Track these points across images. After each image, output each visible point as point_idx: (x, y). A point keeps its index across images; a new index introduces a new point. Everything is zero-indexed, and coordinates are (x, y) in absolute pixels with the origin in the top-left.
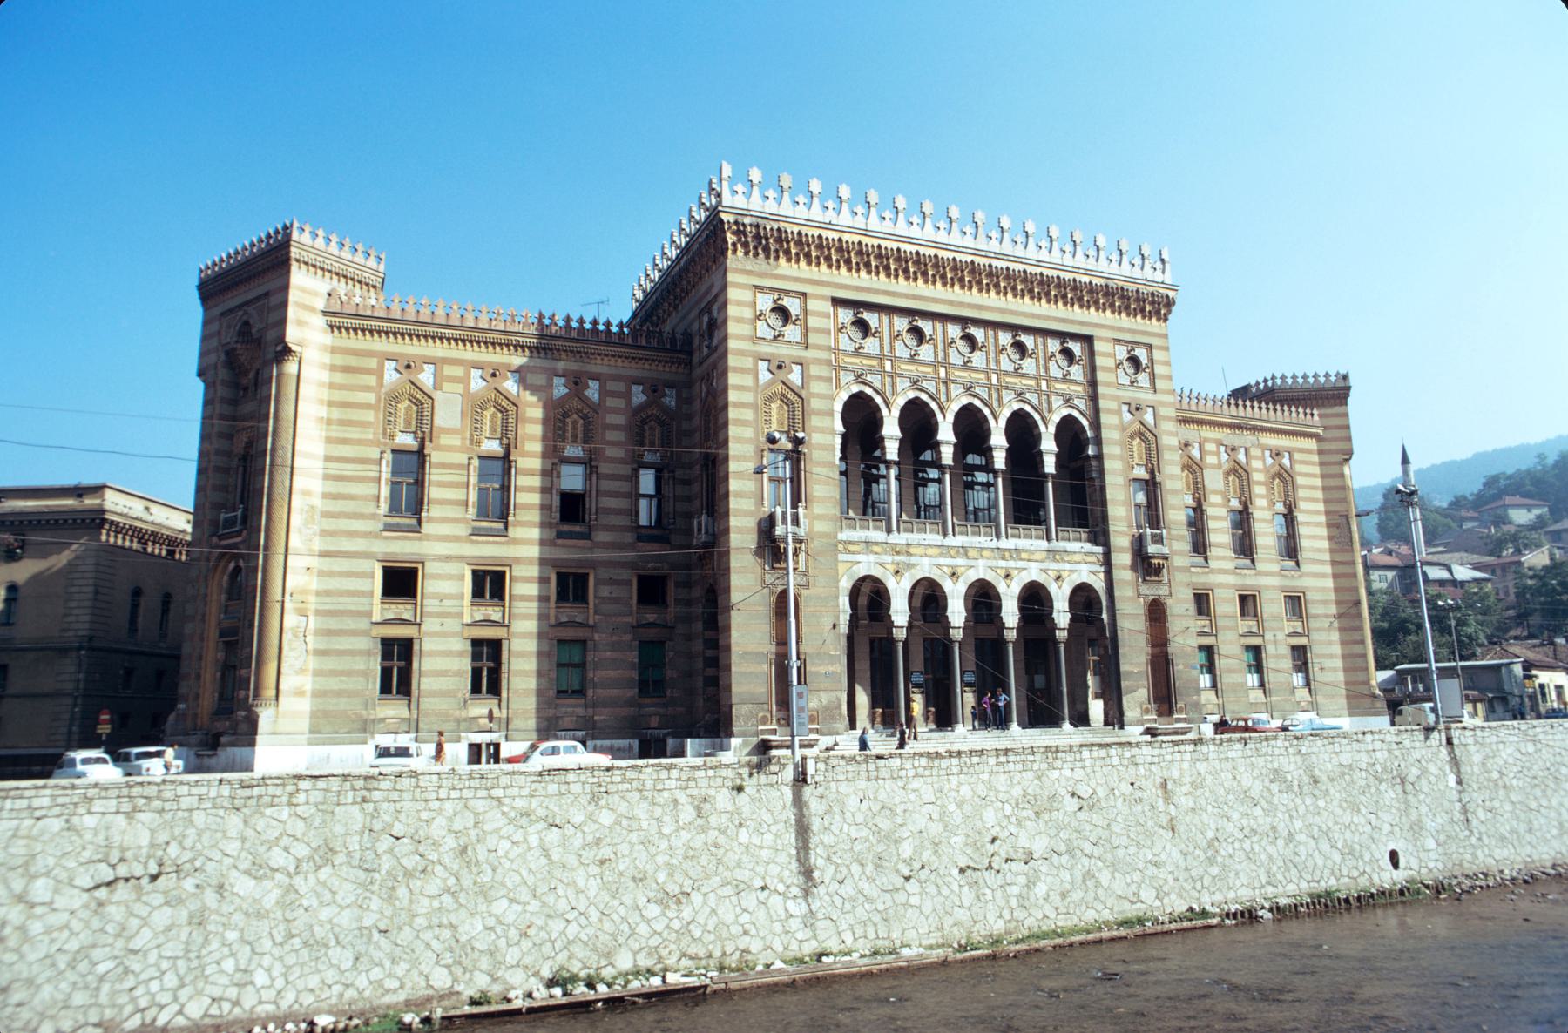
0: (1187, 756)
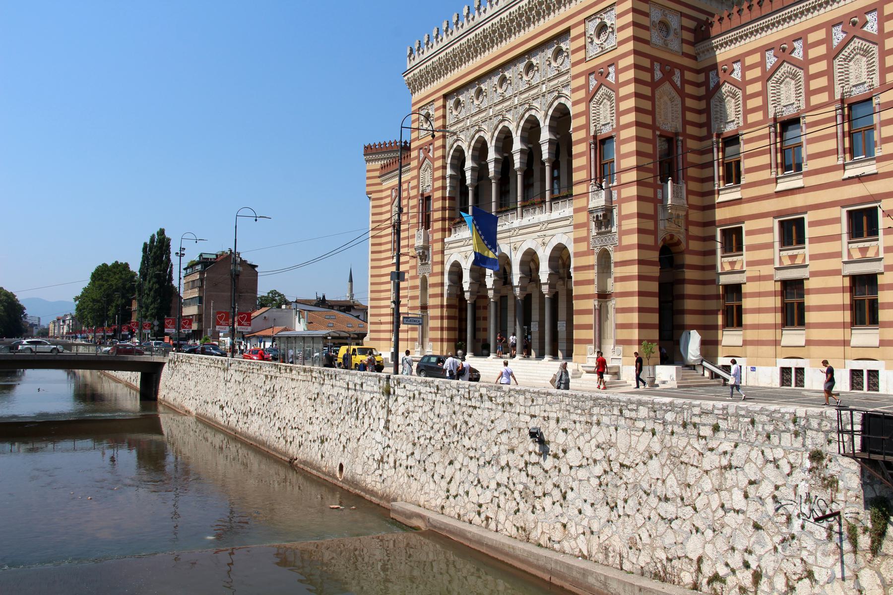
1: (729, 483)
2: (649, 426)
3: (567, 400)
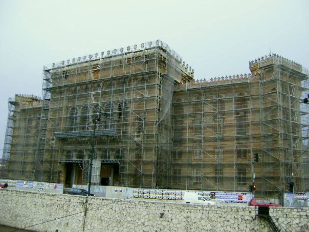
0: (18, 195)
1: (226, 225)
2: (201, 211)
3: (172, 205)
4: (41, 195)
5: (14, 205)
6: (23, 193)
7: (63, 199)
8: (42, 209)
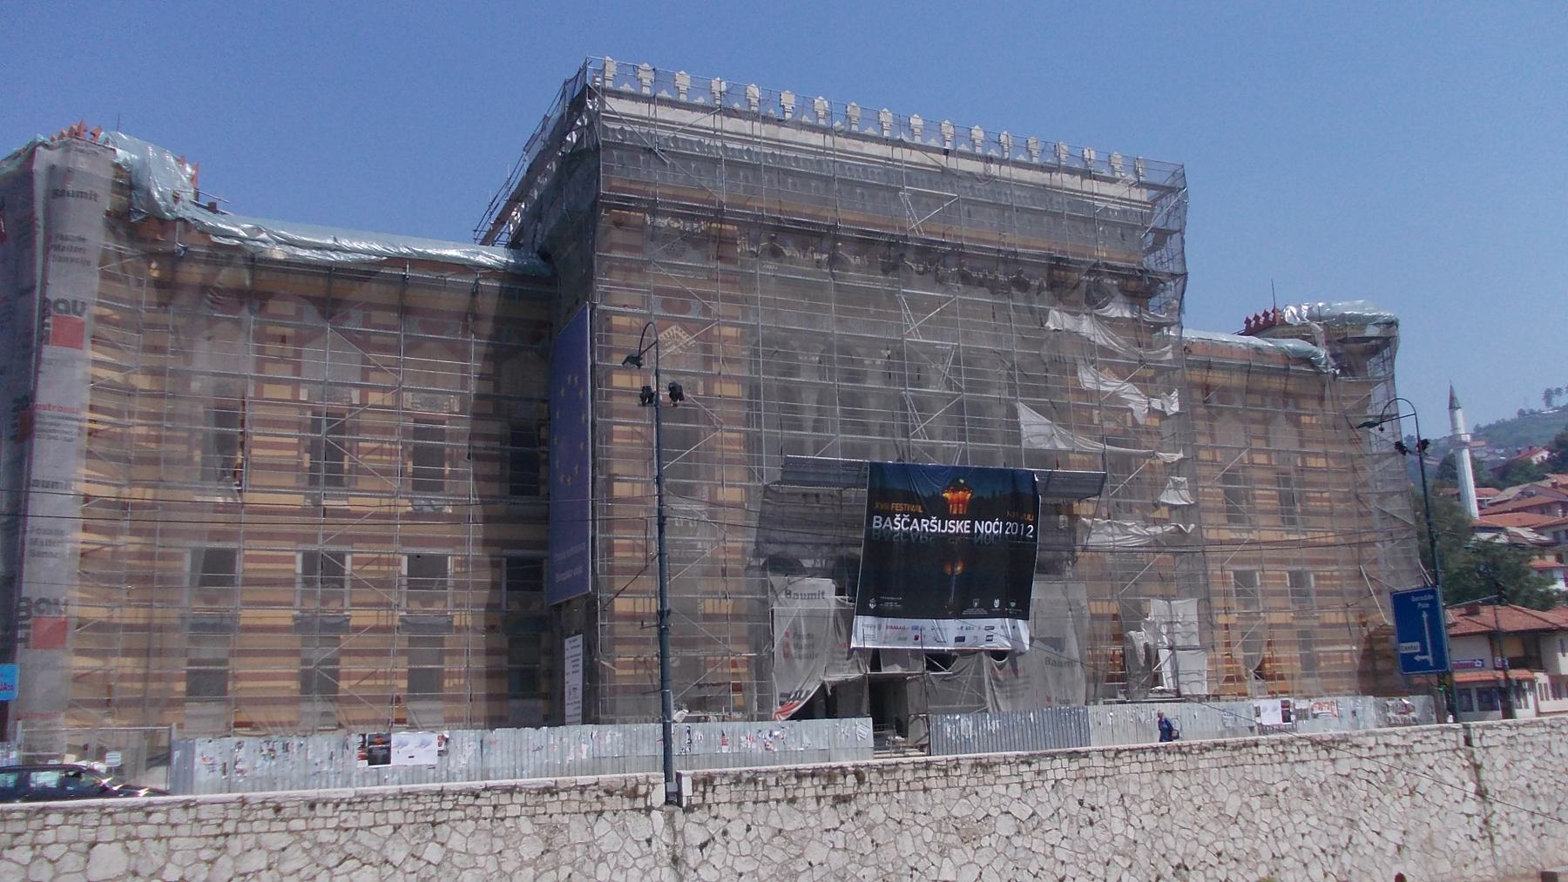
0: (1149, 767)
4: (1281, 748)
5: (1149, 822)
6: (1178, 757)
7: (1382, 750)
8: (1307, 807)
